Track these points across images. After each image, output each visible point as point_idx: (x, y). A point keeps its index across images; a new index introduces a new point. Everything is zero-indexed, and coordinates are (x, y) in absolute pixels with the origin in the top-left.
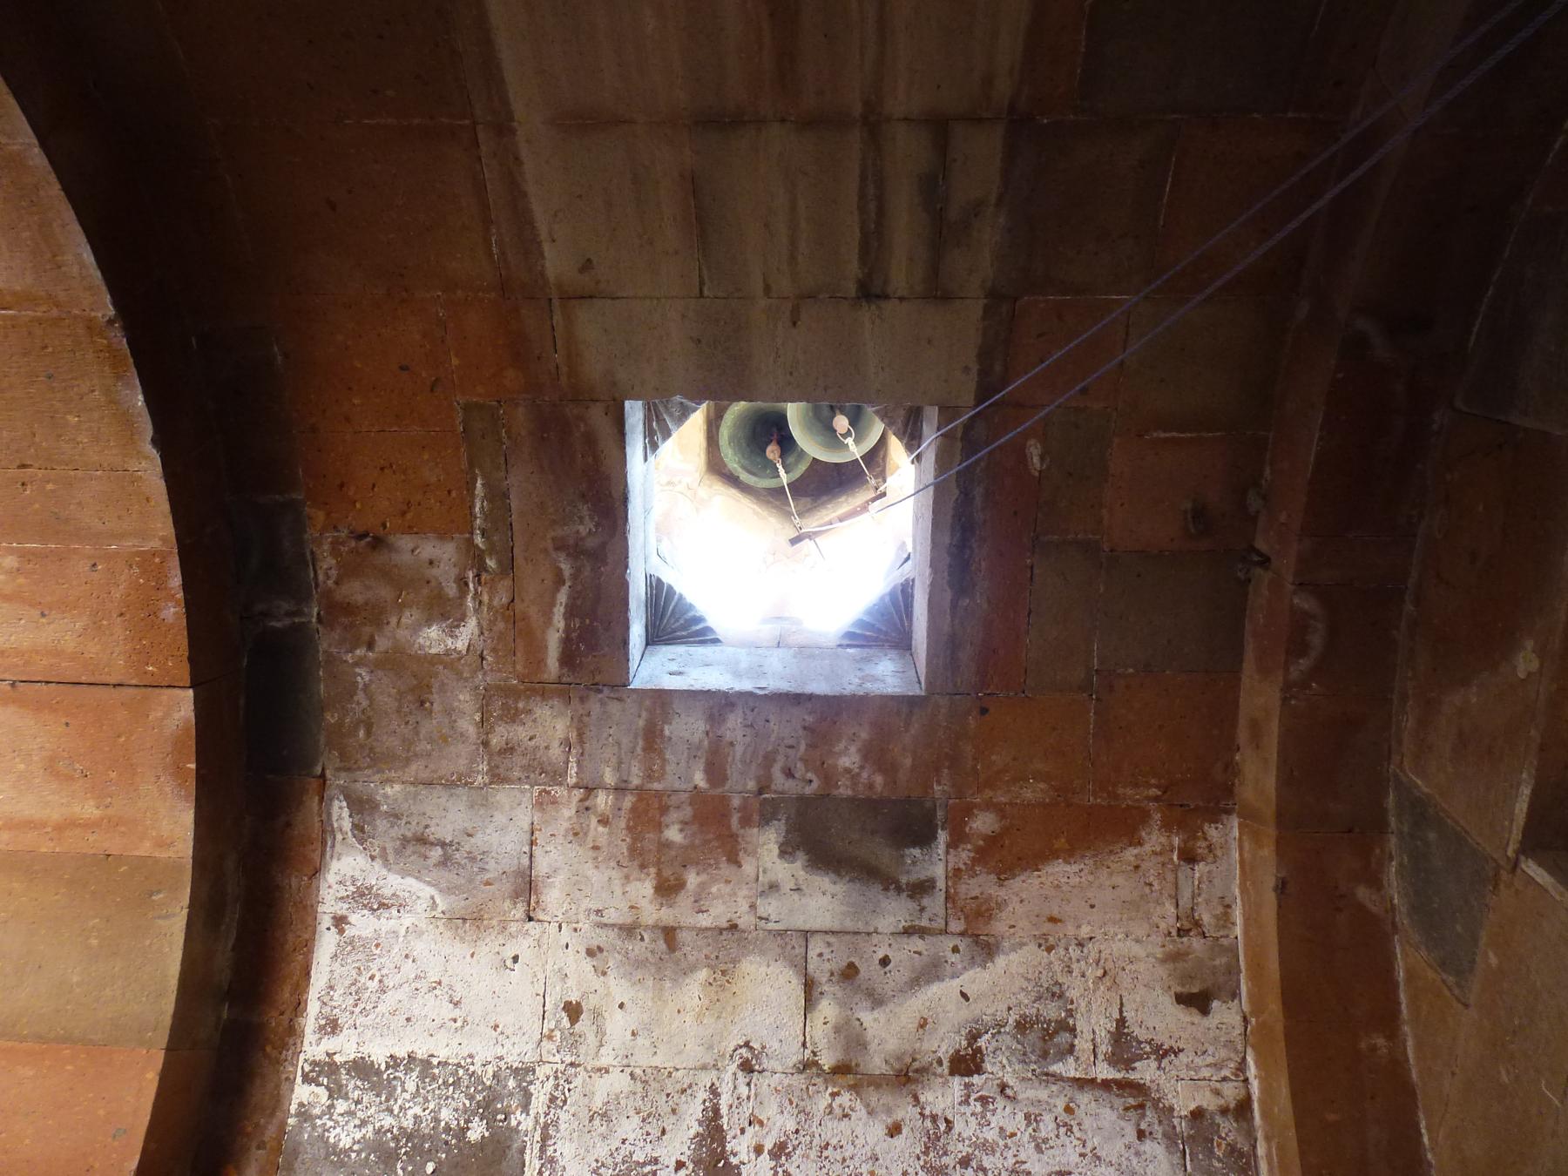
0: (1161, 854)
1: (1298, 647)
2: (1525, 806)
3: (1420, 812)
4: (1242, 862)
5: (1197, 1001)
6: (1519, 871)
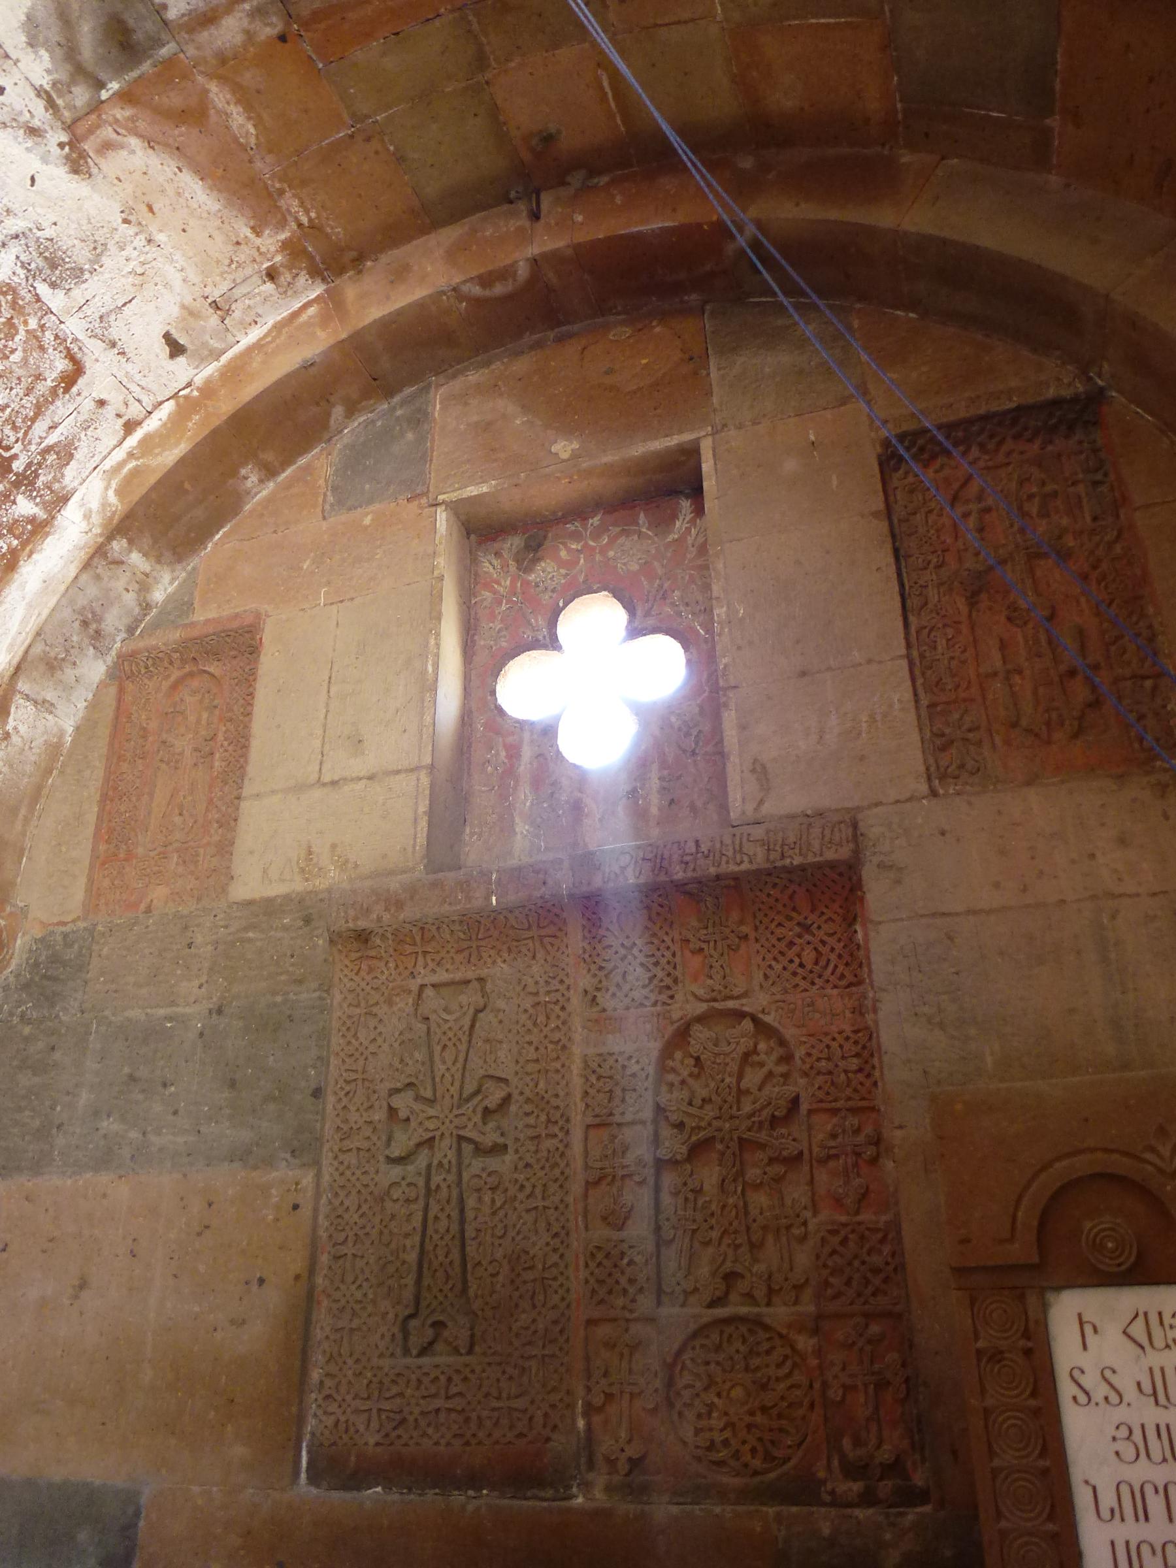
0: (261, 254)
1: (485, 281)
2: (475, 493)
3: (419, 419)
4: (295, 315)
5: (176, 349)
6: (433, 509)
